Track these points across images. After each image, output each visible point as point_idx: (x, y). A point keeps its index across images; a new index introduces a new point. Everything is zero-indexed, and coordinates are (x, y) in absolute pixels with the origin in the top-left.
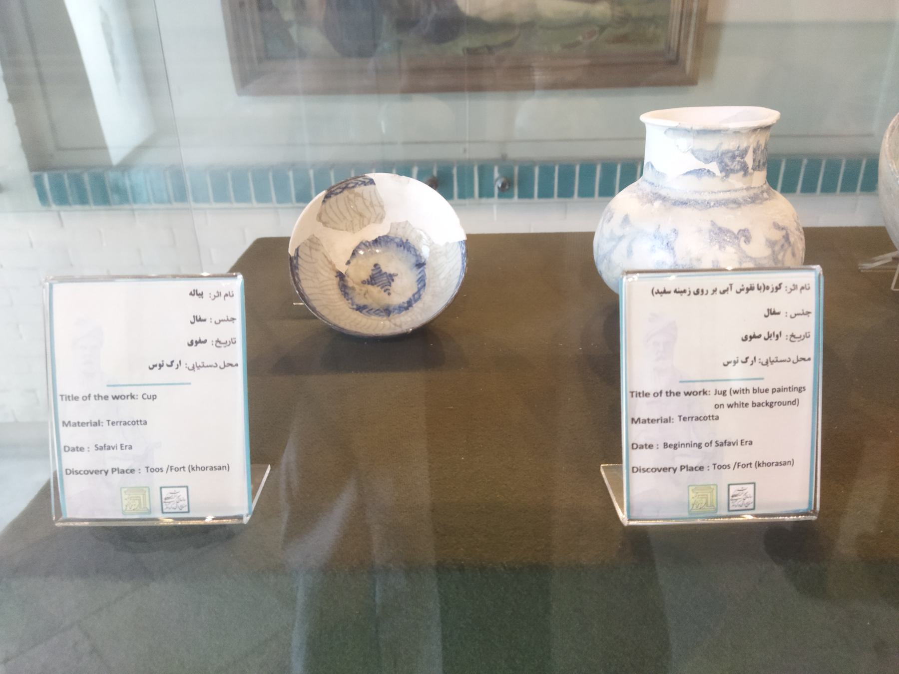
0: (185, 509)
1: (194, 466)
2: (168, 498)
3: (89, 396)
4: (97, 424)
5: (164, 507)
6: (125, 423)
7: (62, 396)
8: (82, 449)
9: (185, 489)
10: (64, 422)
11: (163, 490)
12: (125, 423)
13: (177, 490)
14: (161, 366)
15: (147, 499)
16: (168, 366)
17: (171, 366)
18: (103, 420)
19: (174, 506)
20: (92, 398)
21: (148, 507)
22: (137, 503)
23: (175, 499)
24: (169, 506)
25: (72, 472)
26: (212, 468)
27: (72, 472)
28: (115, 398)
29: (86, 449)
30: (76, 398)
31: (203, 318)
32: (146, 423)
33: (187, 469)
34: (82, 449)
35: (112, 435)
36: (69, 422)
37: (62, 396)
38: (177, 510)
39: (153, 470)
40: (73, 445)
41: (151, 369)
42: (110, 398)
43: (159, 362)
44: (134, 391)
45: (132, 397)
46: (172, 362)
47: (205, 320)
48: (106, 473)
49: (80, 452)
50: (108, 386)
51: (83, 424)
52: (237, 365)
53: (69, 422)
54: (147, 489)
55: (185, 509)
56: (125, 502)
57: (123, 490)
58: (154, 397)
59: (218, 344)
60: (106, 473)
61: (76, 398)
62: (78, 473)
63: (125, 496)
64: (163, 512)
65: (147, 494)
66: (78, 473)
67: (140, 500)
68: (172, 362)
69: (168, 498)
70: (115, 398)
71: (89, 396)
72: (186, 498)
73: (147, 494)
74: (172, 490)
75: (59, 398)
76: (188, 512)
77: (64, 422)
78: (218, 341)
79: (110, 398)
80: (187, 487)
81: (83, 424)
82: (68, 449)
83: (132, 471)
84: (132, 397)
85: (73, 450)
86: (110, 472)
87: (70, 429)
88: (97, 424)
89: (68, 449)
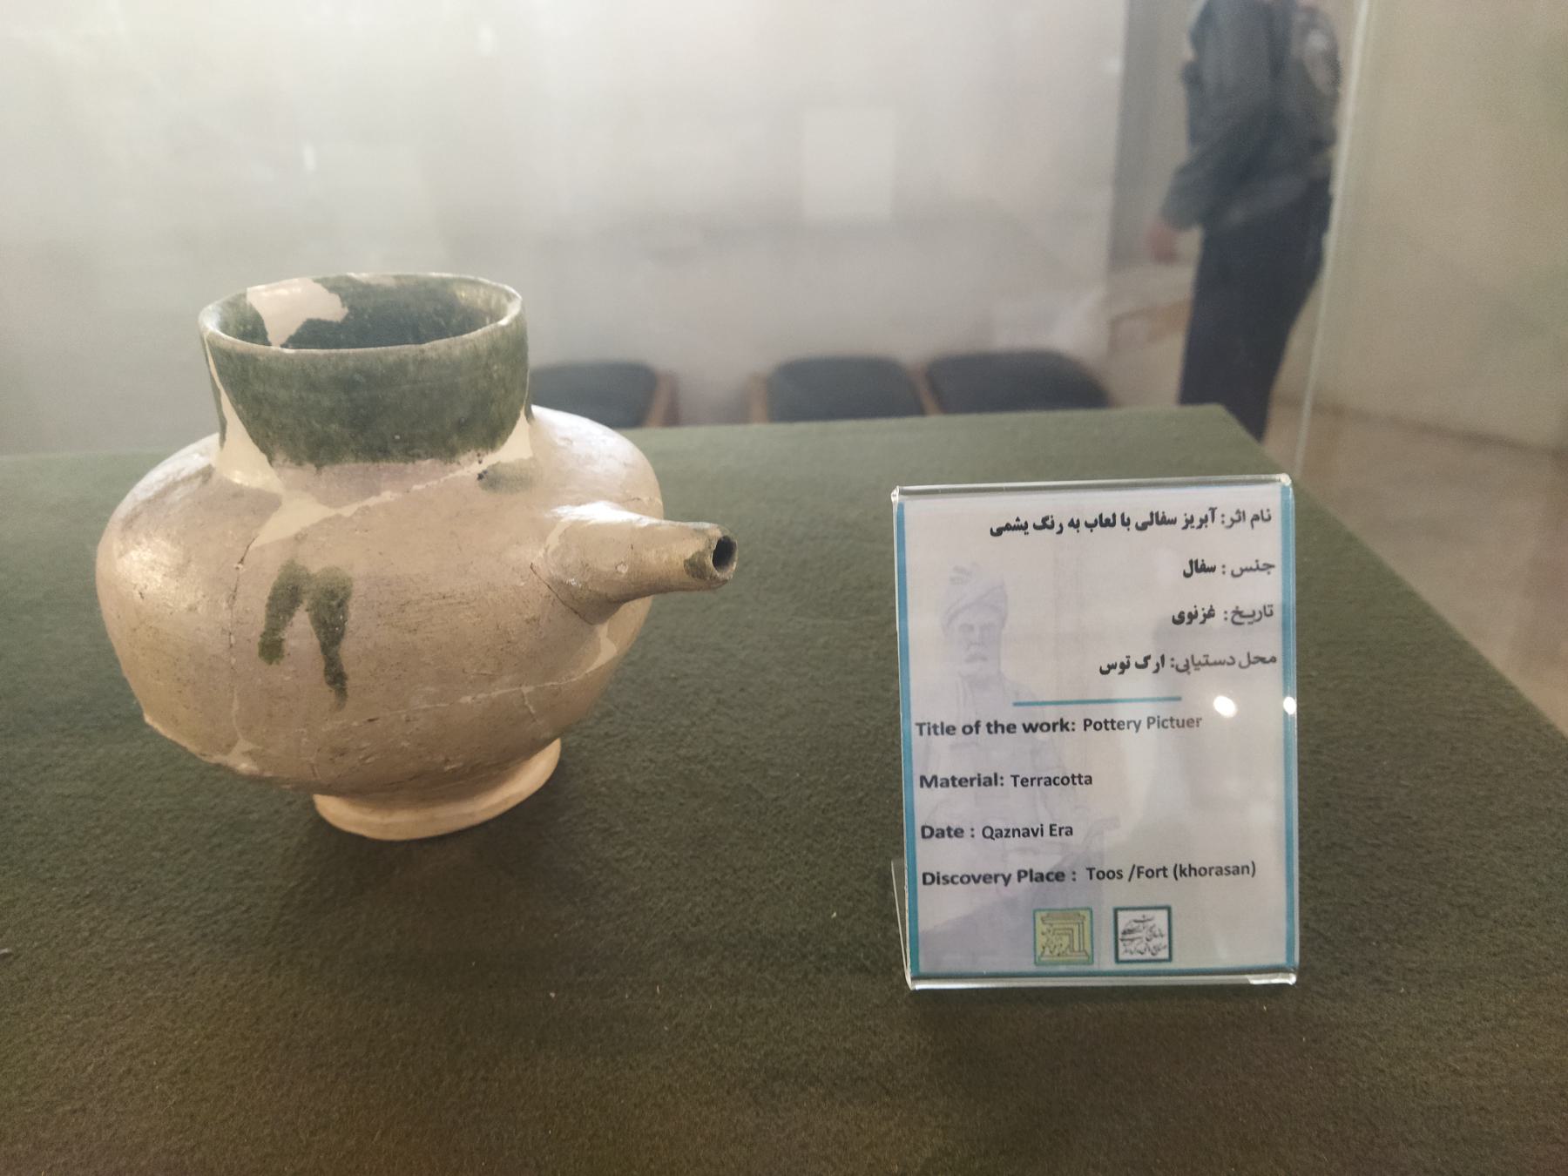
0: (1164, 954)
1: (1185, 866)
2: (1131, 931)
3: (977, 724)
4: (992, 781)
5: (1121, 949)
6: (1050, 782)
7: (921, 725)
8: (959, 833)
9: (1164, 913)
10: (923, 778)
11: (1120, 913)
12: (1050, 782)
13: (1149, 914)
14: (1124, 667)
15: (1087, 933)
16: (1138, 666)
17: (1145, 666)
18: (1006, 774)
19: (1141, 947)
20: (983, 728)
21: (1088, 948)
22: (1066, 940)
23: (1144, 934)
25: (936, 879)
26: (1220, 871)
27: (936, 879)
28: (1029, 728)
29: (967, 833)
30: (950, 730)
31: (1208, 565)
32: (1089, 780)
33: (1170, 873)
34: (959, 833)
35: (1014, 807)
36: (935, 778)
37: (921, 725)
38: (1148, 956)
39: (1102, 875)
40: (940, 823)
41: (1103, 672)
43: (1119, 659)
44: (1074, 715)
45: (1064, 726)
46: (1147, 658)
47: (1213, 570)
48: (1007, 880)
49: (955, 839)
50: (1016, 704)
51: (963, 782)
52: (1273, 660)
53: (935, 778)
54: (1086, 914)
55: (1164, 954)
56: (1041, 940)
57: (1039, 915)
59: (1237, 619)
60: (1007, 880)
61: (950, 730)
62: (949, 880)
63: (1041, 927)
64: (1117, 960)
65: (1087, 923)
66: (949, 880)
68: (1147, 658)
69: (1131, 931)
70: (1029, 728)
71: (977, 724)
72: (1165, 931)
73: (1087, 923)
74: (1138, 915)
75: (915, 730)
76: (1170, 959)
77: (923, 778)
78: (1237, 612)
79: (1020, 729)
80: (1169, 909)
81: (963, 782)
82: (931, 832)
83: (1060, 876)
84: (1064, 726)
85: (941, 834)
86: (1015, 876)
87: (939, 793)
88: (992, 781)
89: (931, 832)
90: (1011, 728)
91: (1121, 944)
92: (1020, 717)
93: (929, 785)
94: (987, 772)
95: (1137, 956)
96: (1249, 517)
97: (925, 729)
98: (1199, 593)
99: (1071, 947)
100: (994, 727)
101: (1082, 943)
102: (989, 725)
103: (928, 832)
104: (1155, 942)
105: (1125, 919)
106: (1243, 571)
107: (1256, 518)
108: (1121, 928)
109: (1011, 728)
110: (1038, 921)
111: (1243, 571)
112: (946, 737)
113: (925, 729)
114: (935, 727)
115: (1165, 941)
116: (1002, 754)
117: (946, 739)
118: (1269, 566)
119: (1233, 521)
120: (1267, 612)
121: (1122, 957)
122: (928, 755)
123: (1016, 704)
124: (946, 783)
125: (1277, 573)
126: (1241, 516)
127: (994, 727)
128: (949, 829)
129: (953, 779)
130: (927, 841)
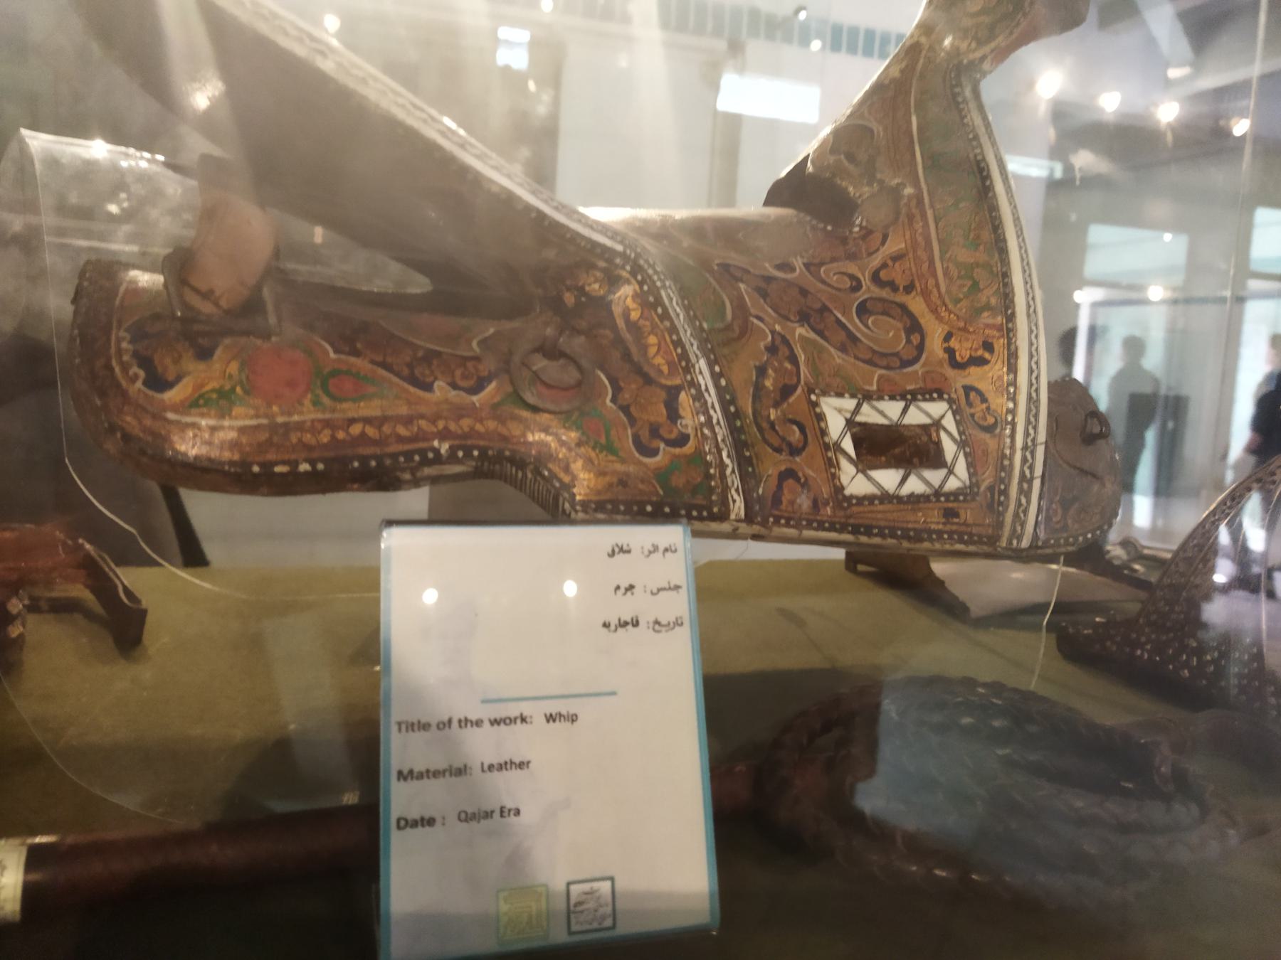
3: (450, 721)
5: (573, 921)
7: (399, 724)
8: (430, 822)
10: (400, 773)
13: (596, 885)
28: (495, 722)
29: (439, 821)
34: (430, 822)
36: (411, 772)
37: (399, 724)
38: (595, 925)
40: (414, 814)
45: (523, 720)
49: (427, 829)
50: (484, 701)
51: (436, 774)
53: (411, 772)
55: (608, 923)
57: (502, 895)
58: (573, 718)
59: (657, 627)
61: (425, 727)
64: (570, 933)
70: (495, 722)
71: (450, 721)
75: (394, 728)
76: (614, 927)
77: (400, 773)
78: (657, 622)
79: (487, 724)
80: (612, 879)
81: (436, 774)
82: (405, 824)
84: (523, 720)
85: (414, 824)
87: (413, 785)
89: (405, 824)
90: (478, 723)
91: (572, 916)
93: (405, 779)
97: (404, 727)
98: (625, 608)
102: (460, 721)
103: (403, 823)
106: (659, 590)
107: (666, 550)
108: (573, 902)
109: (478, 723)
110: (502, 903)
111: (659, 590)
112: (422, 733)
113: (404, 727)
114: (413, 724)
117: (419, 736)
118: (677, 587)
119: (650, 552)
120: (678, 623)
123: (484, 701)
124: (420, 776)
125: (683, 592)
126: (655, 548)
128: (422, 819)
129: (428, 771)
130: (402, 832)
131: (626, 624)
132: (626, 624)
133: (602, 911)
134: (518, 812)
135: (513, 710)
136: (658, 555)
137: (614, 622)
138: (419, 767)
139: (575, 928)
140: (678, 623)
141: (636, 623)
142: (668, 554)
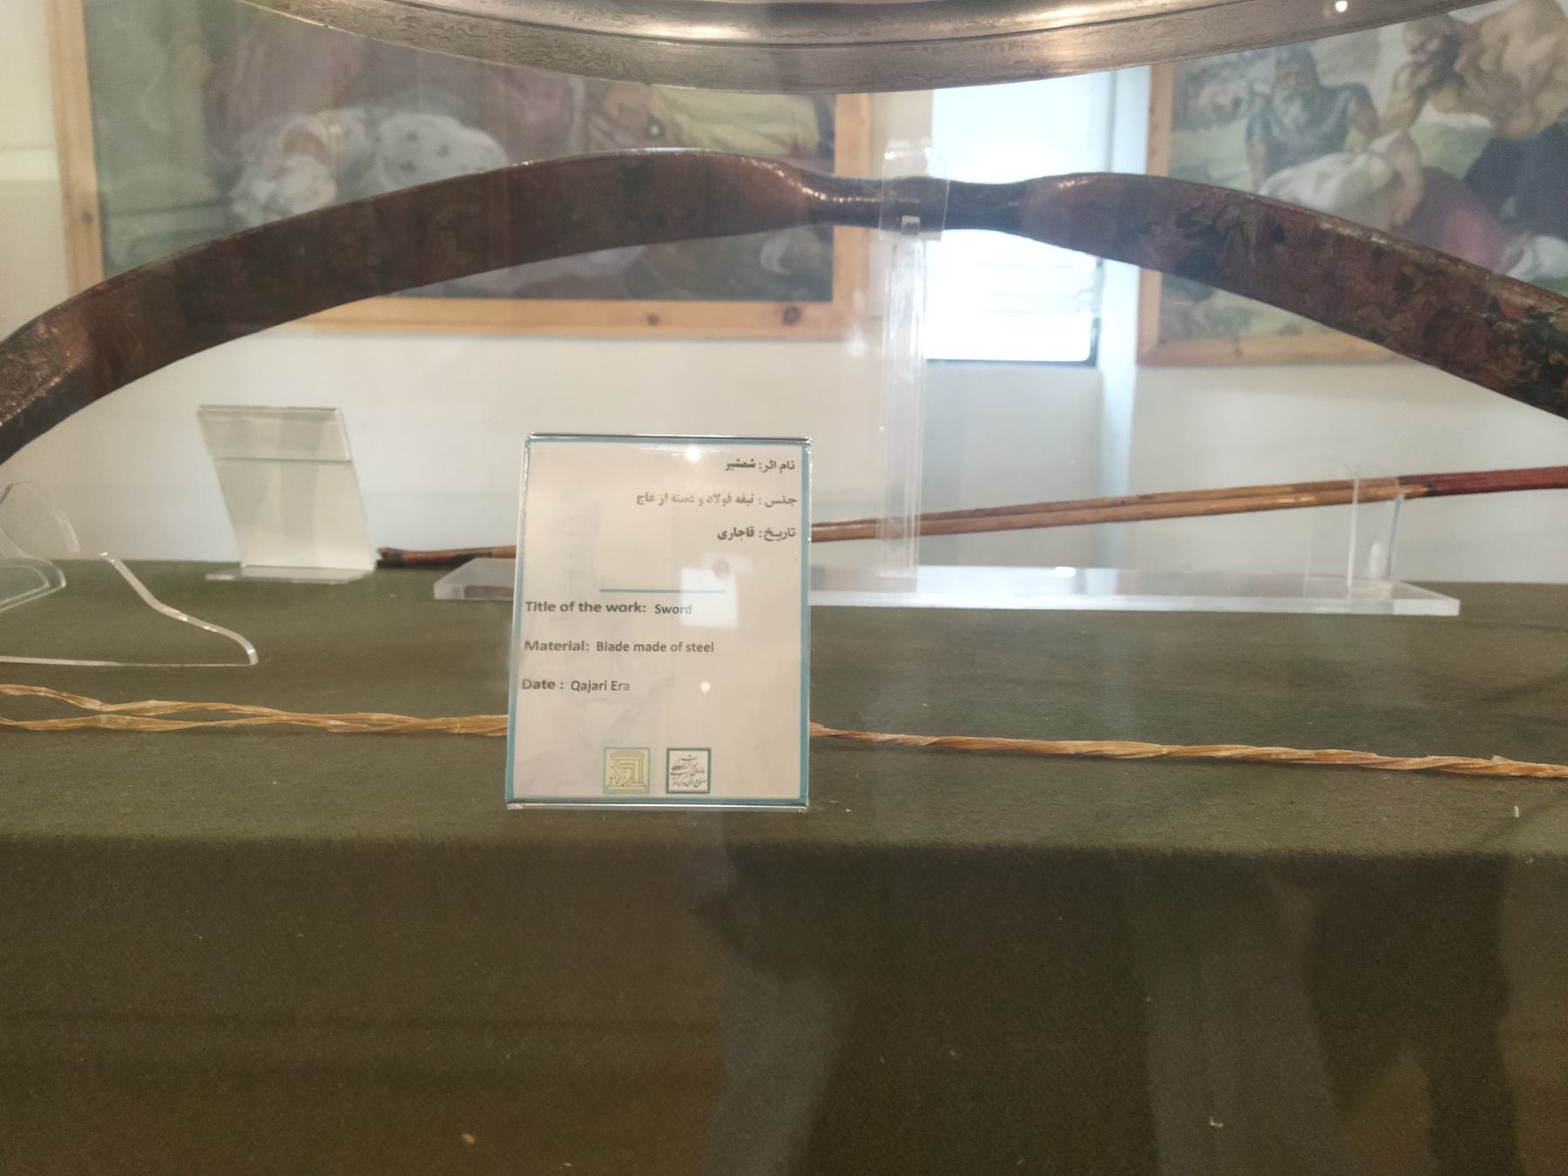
4: (579, 647)
8: (551, 685)
10: (527, 643)
13: (694, 754)
19: (687, 780)
20: (576, 608)
23: (689, 770)
24: (679, 780)
28: (611, 608)
29: (558, 685)
30: (551, 608)
34: (551, 685)
38: (691, 788)
42: (604, 609)
44: (641, 599)
45: (637, 608)
51: (557, 647)
55: (704, 787)
56: (610, 773)
61: (551, 608)
67: (633, 770)
70: (611, 608)
74: (686, 754)
75: (525, 607)
78: (769, 532)
79: (604, 609)
80: (709, 750)
81: (557, 647)
85: (537, 685)
88: (579, 647)
90: (597, 608)
92: (605, 600)
94: (577, 640)
95: (683, 788)
96: (779, 464)
98: (740, 517)
99: (632, 778)
100: (584, 607)
101: (641, 776)
104: (697, 777)
105: (675, 757)
107: (784, 466)
109: (597, 608)
115: (705, 776)
116: (590, 628)
120: (790, 534)
121: (671, 788)
122: (529, 625)
124: (545, 647)
125: (798, 504)
126: (773, 464)
127: (584, 607)
131: (742, 533)
132: (742, 533)
133: (697, 777)
134: (627, 687)
135: (628, 600)
136: (776, 471)
137: (730, 531)
138: (544, 640)
139: (671, 788)
140: (790, 534)
141: (750, 533)
142: (785, 471)
